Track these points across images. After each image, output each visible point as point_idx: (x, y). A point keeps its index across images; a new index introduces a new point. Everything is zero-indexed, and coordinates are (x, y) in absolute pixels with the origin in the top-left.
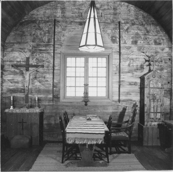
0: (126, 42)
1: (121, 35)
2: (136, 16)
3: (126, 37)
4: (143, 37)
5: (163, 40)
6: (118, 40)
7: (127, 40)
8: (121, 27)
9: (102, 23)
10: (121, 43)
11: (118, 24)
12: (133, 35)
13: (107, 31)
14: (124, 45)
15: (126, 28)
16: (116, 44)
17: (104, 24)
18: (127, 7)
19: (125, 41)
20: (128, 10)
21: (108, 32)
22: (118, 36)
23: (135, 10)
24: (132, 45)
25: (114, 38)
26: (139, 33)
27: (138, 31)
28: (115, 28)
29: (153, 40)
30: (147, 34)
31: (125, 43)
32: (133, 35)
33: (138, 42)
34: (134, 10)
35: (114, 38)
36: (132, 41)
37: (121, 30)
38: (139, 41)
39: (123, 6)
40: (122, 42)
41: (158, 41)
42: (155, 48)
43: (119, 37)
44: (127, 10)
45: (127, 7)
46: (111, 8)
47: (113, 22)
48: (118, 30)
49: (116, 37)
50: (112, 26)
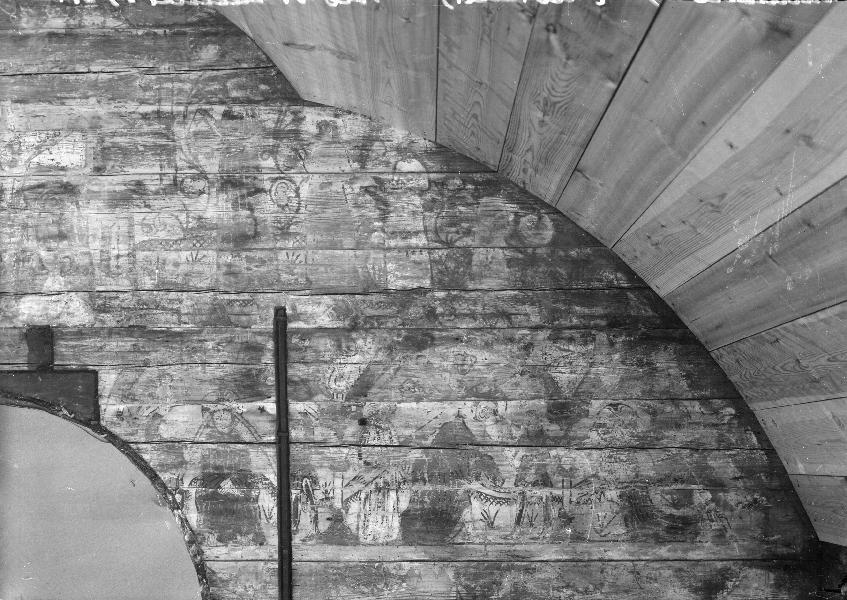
0: (351, 521)
1: (294, 450)
2: (449, 244)
3: (350, 474)
4: (511, 460)
5: (716, 485)
6: (268, 502)
7: (355, 506)
8: (297, 371)
9: (111, 332)
10: (296, 540)
11: (270, 345)
12: (415, 455)
13: (156, 416)
14: (330, 552)
15: (347, 370)
16: (245, 550)
17: (126, 344)
18: (362, 160)
19: (337, 519)
20: (366, 190)
21: (166, 432)
22: (263, 463)
23: (442, 184)
24: (411, 552)
25: (227, 487)
26: (473, 427)
27: (467, 408)
28: (248, 387)
29: (612, 493)
30: (554, 429)
31: (338, 532)
32: (415, 455)
33: (466, 515)
34: (423, 182)
35: (227, 487)
36: (404, 505)
37: (296, 407)
38: (475, 510)
39: (314, 150)
40: (305, 523)
41: (658, 498)
42: (635, 572)
43: (273, 478)
44: (357, 187)
45: (362, 160)
46: (203, 175)
47: (219, 318)
48: (271, 407)
49: (245, 479)
50: (217, 363)
